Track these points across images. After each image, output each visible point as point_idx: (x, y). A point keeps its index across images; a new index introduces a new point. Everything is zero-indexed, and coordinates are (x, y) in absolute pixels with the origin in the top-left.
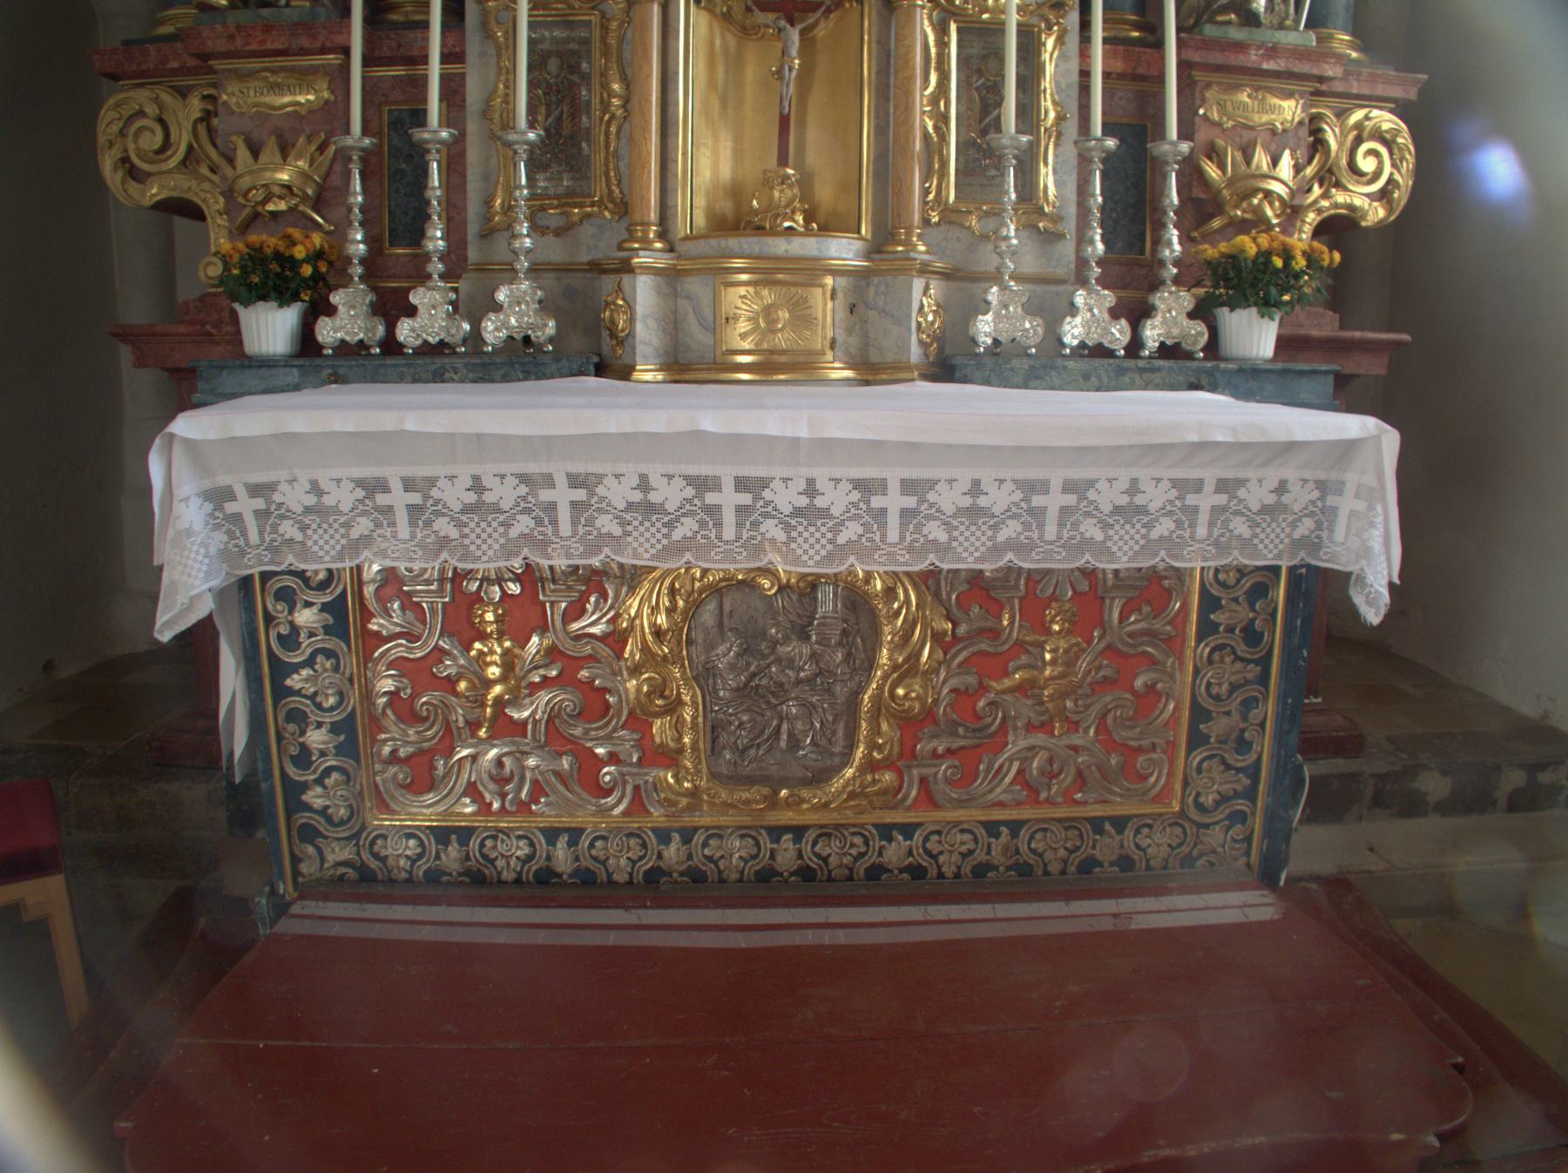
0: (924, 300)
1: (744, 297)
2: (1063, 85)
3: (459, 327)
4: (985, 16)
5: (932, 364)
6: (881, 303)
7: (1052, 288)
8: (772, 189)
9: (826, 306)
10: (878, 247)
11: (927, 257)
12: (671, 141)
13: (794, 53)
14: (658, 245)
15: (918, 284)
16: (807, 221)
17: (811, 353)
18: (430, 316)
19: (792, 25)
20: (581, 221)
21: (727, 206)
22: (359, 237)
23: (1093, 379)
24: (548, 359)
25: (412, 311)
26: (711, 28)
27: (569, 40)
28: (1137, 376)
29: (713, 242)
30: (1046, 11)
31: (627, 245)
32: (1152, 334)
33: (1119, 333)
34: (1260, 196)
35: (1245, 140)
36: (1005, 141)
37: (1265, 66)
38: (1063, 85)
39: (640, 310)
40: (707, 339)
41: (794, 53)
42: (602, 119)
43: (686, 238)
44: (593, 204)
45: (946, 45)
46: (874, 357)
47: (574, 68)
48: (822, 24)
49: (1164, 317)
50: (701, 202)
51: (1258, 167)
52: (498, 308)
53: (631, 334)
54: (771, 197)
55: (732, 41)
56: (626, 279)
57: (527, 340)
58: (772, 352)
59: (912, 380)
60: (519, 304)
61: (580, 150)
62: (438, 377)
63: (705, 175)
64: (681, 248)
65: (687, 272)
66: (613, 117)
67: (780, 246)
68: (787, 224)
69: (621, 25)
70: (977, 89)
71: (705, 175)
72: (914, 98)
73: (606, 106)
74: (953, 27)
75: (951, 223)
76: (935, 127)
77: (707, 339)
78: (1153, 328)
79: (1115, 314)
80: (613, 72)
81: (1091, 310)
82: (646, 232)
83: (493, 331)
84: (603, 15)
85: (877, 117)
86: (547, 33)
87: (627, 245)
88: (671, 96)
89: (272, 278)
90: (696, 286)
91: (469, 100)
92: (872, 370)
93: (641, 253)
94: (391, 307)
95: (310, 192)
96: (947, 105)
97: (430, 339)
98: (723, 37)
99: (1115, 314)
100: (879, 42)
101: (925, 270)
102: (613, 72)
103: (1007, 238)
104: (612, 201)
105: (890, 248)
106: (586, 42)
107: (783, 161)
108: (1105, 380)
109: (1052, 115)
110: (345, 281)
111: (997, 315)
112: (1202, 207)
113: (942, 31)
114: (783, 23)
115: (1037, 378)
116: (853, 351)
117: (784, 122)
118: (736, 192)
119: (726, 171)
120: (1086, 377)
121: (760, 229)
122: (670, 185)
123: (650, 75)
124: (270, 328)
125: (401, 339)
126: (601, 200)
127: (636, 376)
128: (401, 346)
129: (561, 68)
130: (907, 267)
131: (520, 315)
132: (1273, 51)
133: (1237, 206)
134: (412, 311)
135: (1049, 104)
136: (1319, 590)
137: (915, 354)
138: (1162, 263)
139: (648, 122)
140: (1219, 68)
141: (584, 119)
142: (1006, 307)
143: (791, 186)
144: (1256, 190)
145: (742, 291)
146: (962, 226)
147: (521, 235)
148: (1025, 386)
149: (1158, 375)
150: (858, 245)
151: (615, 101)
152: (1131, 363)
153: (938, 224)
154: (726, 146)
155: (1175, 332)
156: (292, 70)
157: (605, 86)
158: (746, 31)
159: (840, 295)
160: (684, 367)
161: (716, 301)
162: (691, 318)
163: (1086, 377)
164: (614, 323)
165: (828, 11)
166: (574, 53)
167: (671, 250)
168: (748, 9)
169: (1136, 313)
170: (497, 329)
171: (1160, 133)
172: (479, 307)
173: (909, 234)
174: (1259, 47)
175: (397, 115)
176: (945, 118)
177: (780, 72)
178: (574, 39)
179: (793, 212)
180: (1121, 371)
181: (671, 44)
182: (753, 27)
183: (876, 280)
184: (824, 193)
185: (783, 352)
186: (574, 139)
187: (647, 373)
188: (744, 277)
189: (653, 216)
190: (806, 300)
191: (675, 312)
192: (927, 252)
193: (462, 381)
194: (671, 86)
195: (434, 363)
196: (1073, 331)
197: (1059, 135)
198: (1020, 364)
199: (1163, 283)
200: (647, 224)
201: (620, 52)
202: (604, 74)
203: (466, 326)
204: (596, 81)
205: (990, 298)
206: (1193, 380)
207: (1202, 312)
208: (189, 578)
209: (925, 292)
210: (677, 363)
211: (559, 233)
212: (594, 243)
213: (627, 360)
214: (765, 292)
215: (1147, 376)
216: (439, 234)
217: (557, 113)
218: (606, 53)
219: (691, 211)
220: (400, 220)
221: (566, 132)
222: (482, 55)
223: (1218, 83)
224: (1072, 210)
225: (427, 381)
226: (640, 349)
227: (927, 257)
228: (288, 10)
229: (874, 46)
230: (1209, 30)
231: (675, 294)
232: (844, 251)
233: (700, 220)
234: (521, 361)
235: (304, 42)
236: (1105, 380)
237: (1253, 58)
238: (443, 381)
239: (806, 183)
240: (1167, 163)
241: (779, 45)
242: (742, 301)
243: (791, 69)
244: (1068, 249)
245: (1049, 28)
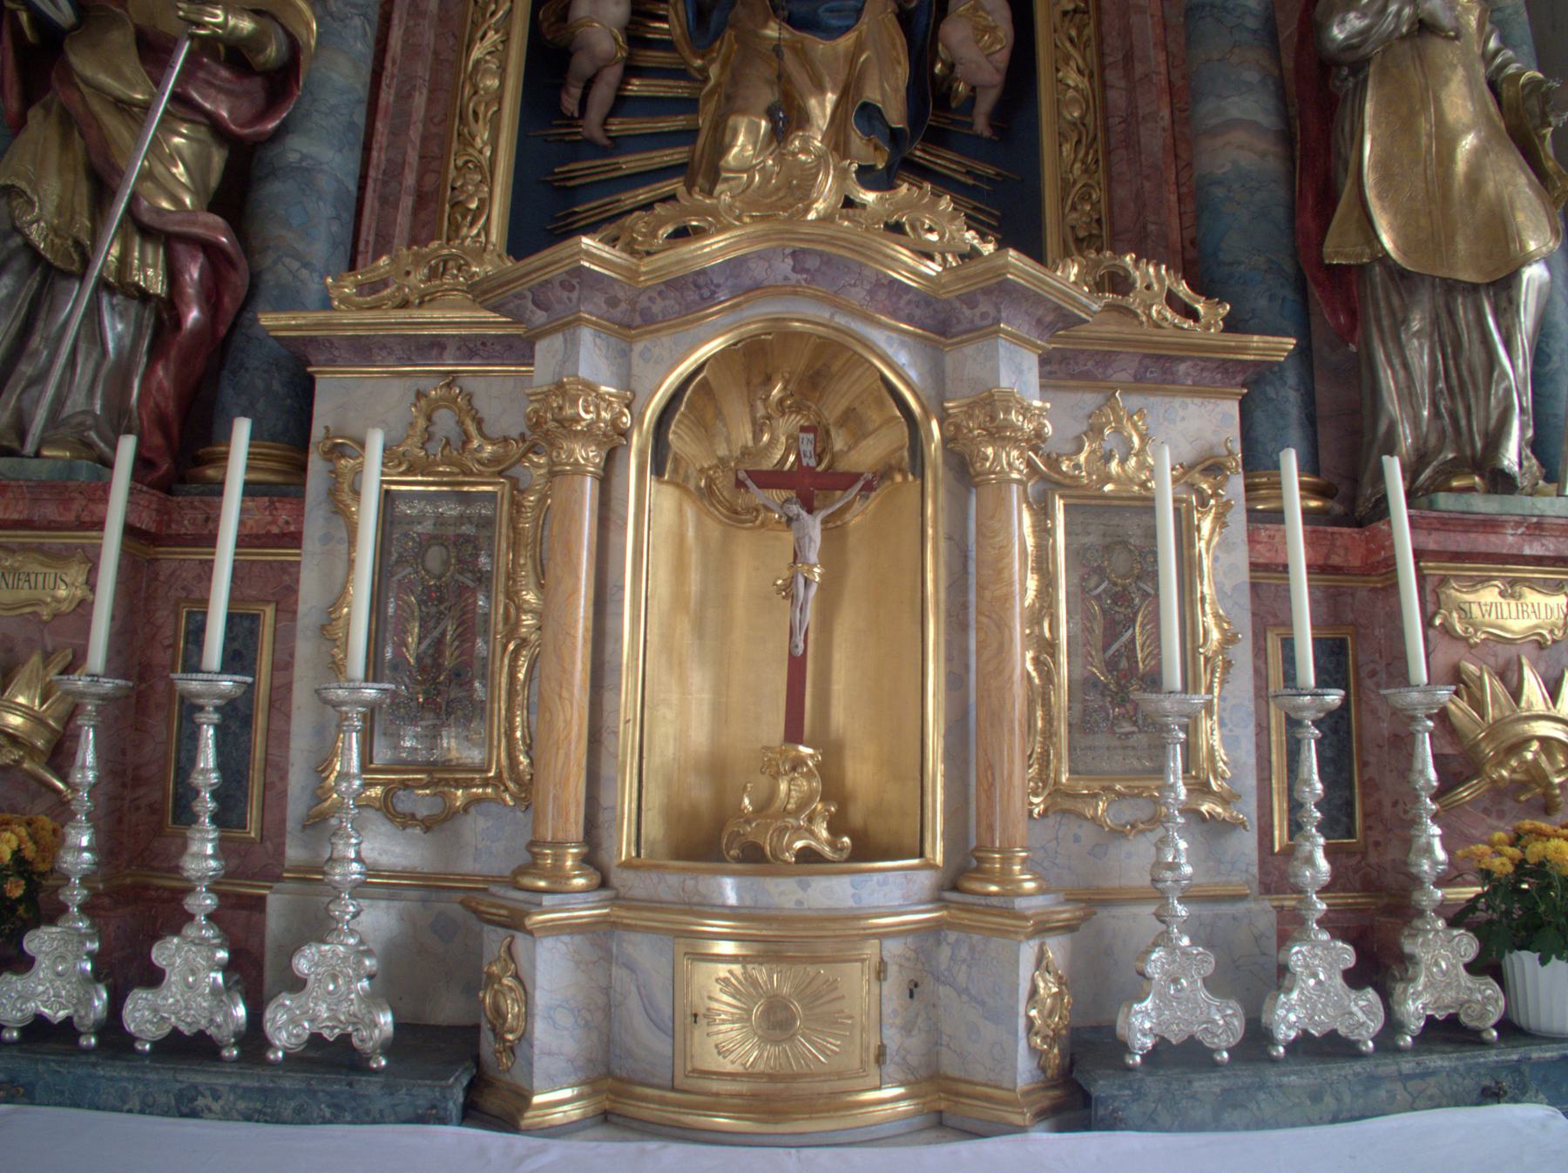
1: (726, 981)
2: (1228, 589)
3: (228, 1015)
4: (1109, 487)
5: (1051, 1084)
6: (962, 978)
7: (1226, 909)
8: (776, 776)
10: (957, 880)
11: (1040, 901)
12: (608, 696)
13: (813, 557)
14: (579, 882)
15: (1028, 952)
16: (835, 829)
17: (840, 1076)
18: (191, 981)
19: (810, 511)
20: (466, 809)
21: (700, 793)
22: (85, 841)
23: (1328, 1099)
24: (370, 1088)
25: (154, 978)
26: (680, 512)
27: (462, 519)
28: (1398, 1087)
29: (673, 880)
30: (1196, 476)
31: (526, 881)
32: (1415, 1006)
33: (1361, 1013)
34: (1535, 746)
35: (1501, 661)
36: (1167, 704)
37: (1527, 551)
38: (1228, 589)
39: (541, 998)
40: (662, 1046)
41: (813, 557)
42: (505, 647)
43: (627, 866)
44: (486, 783)
45: (1050, 532)
46: (949, 1065)
47: (467, 564)
48: (857, 506)
49: (1430, 974)
50: (655, 798)
51: (1530, 705)
52: (297, 984)
53: (525, 1037)
54: (774, 791)
55: (714, 531)
56: (521, 941)
57: (345, 1039)
58: (771, 1077)
59: (1021, 1129)
60: (334, 978)
61: (472, 690)
62: (186, 1107)
63: (664, 748)
64: (618, 877)
65: (628, 927)
66: (524, 643)
67: (784, 893)
68: (799, 844)
69: (542, 499)
70: (1098, 597)
71: (664, 748)
72: (1011, 629)
73: (512, 626)
74: (1059, 504)
75: (1064, 812)
76: (1037, 661)
77: (662, 1046)
78: (1417, 995)
79: (1354, 979)
80: (526, 574)
81: (1315, 975)
82: (560, 858)
83: (286, 1027)
84: (515, 483)
85: (949, 659)
86: (429, 509)
87: (526, 881)
88: (610, 624)
90: (641, 950)
91: (302, 608)
92: (951, 1109)
93: (547, 900)
95: (40, 743)
96: (1054, 628)
97: (183, 1027)
98: (699, 525)
99: (1354, 979)
100: (950, 538)
101: (1043, 929)
102: (526, 574)
103: (1174, 867)
104: (518, 781)
105: (976, 886)
106: (488, 523)
107: (794, 733)
108: (1347, 1098)
109: (1215, 635)
110: (53, 913)
111: (1162, 996)
113: (1042, 512)
114: (795, 509)
115: (1235, 1107)
116: (913, 1060)
117: (796, 667)
118: (717, 768)
119: (699, 736)
120: (1316, 1097)
121: (755, 858)
122: (606, 769)
123: (576, 590)
125: (131, 1028)
126: (499, 774)
127: (529, 1118)
128: (132, 1039)
129: (446, 563)
130: (1004, 919)
131: (336, 998)
132: (1537, 527)
133: (1501, 764)
134: (154, 978)
135: (1210, 621)
137: (1024, 1070)
138: (1416, 881)
139: (566, 672)
140: (1457, 557)
141: (479, 643)
142: (1176, 981)
143: (809, 775)
144: (1526, 741)
145: (722, 970)
146: (1081, 816)
147: (346, 860)
148: (1216, 1125)
149: (1432, 1080)
150: (925, 881)
151: (528, 620)
152: (1388, 1067)
153: (1043, 815)
154: (699, 680)
155: (1449, 996)
156: (40, 549)
157: (512, 595)
158: (736, 516)
159: (893, 970)
160: (624, 1099)
161: (676, 984)
162: (634, 1002)
163: (1316, 1097)
164: (499, 1013)
165: (869, 487)
166: (467, 539)
167: (604, 884)
168: (740, 484)
170: (295, 1021)
171: (1398, 671)
173: (1007, 861)
174: (1518, 525)
176: (1050, 647)
177: (789, 590)
178: (470, 519)
179: (810, 819)
180: (1373, 1081)
181: (613, 538)
182: (748, 511)
183: (952, 936)
184: (861, 773)
185: (795, 1077)
186: (460, 676)
187: (557, 1100)
188: (727, 948)
189: (576, 829)
190: (832, 985)
191: (607, 991)
192: (1041, 891)
193: (226, 1116)
194: (611, 608)
196: (1289, 1017)
197: (1228, 665)
198: (1206, 1085)
199: (1420, 913)
200: (559, 845)
201: (539, 541)
202: (511, 576)
203: (240, 1011)
204: (500, 583)
205: (1150, 970)
206: (1487, 1082)
207: (1486, 966)
209: (1041, 961)
210: (609, 1074)
211: (428, 825)
212: (485, 846)
213: (521, 1081)
214: (760, 973)
215: (1413, 1085)
216: (209, 850)
217: (436, 633)
218: (515, 546)
221: (448, 662)
222: (327, 539)
223: (1456, 577)
224: (1251, 781)
225: (166, 1113)
226: (541, 1065)
227: (1040, 901)
228: (36, 461)
229: (942, 544)
230: (1445, 501)
231: (607, 957)
233: (654, 827)
235: (51, 511)
236: (1347, 1098)
237: (1509, 541)
238: (194, 1114)
239: (832, 753)
240: (1413, 718)
241: (789, 537)
243: (807, 583)
244: (1247, 843)
245: (1203, 503)
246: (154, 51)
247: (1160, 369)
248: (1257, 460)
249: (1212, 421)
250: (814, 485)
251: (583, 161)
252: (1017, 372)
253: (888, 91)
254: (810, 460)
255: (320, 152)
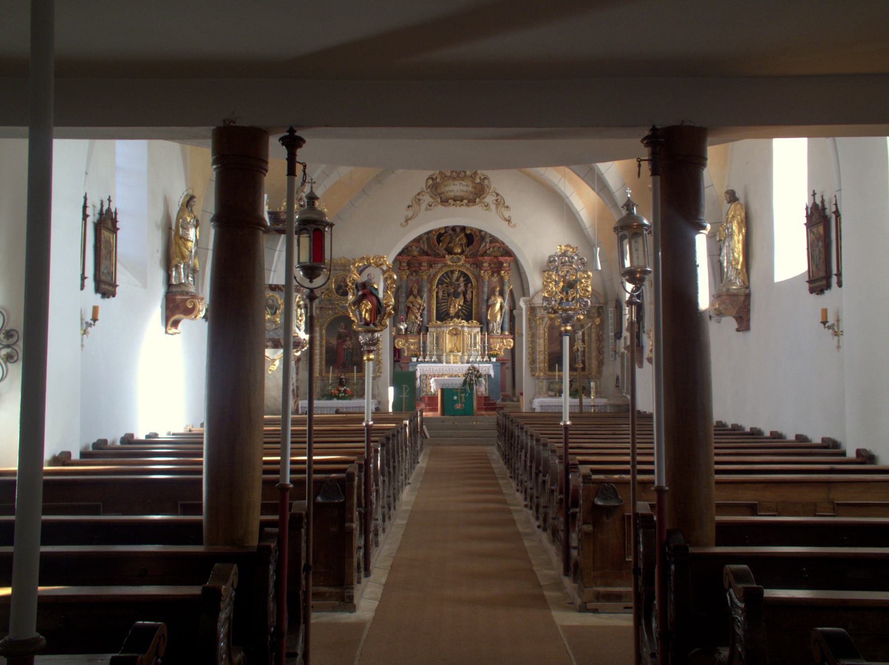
0: (466, 357)
9: (458, 358)
18: (427, 359)
89: (416, 356)
94: (424, 358)
112: (490, 349)
124: (414, 359)
136: (489, 376)
169: (483, 358)
172: (431, 358)
175: (424, 343)
195: (428, 362)
208: (418, 374)
212: (440, 353)
219: (448, 350)
220: (424, 351)
232: (460, 354)
234: (435, 362)
242: (452, 357)
246: (419, 309)
247: (475, 327)
248: (481, 331)
249: (479, 329)
250: (456, 334)
251: (443, 316)
252: (466, 329)
253: (462, 303)
254: (456, 333)
255: (425, 312)
